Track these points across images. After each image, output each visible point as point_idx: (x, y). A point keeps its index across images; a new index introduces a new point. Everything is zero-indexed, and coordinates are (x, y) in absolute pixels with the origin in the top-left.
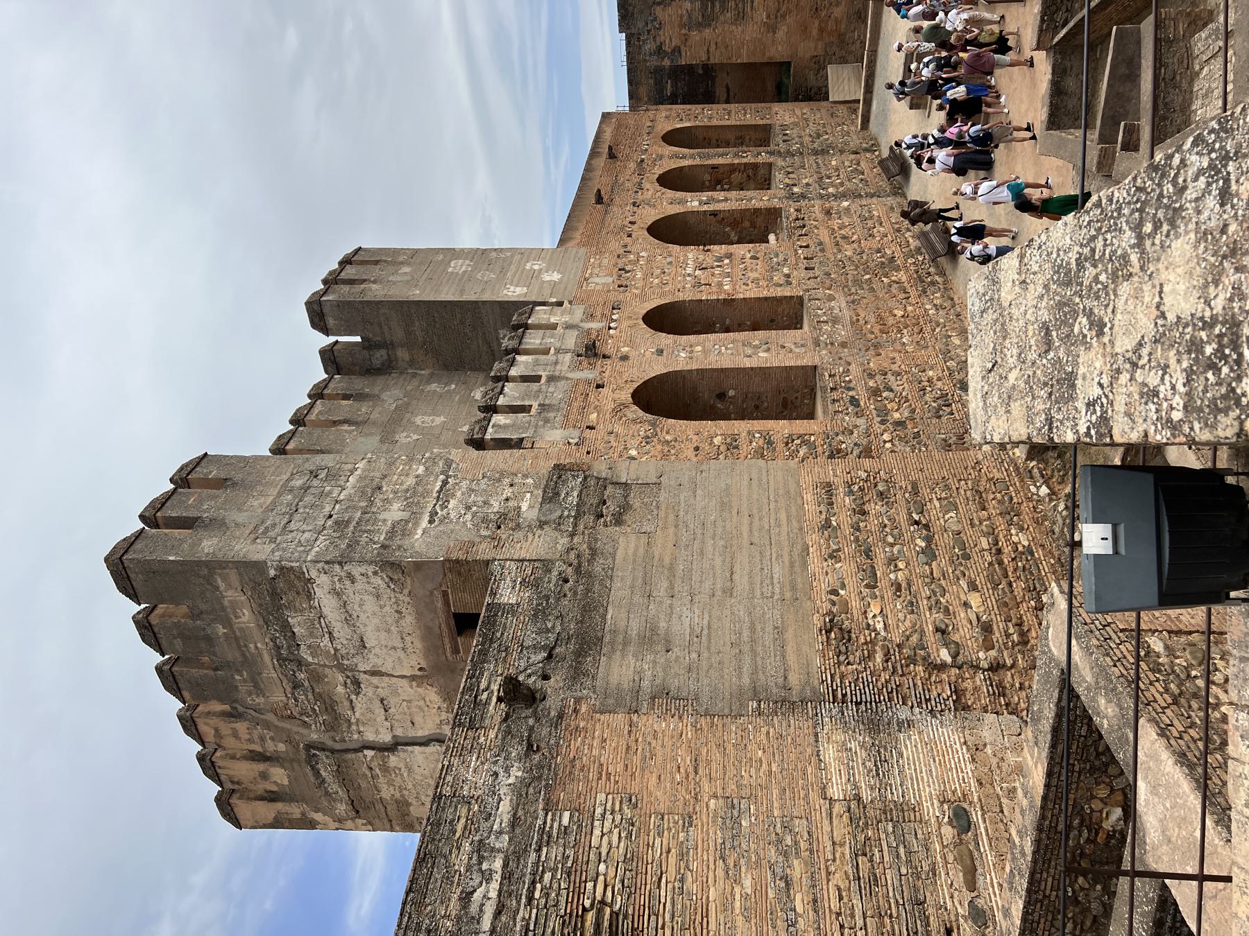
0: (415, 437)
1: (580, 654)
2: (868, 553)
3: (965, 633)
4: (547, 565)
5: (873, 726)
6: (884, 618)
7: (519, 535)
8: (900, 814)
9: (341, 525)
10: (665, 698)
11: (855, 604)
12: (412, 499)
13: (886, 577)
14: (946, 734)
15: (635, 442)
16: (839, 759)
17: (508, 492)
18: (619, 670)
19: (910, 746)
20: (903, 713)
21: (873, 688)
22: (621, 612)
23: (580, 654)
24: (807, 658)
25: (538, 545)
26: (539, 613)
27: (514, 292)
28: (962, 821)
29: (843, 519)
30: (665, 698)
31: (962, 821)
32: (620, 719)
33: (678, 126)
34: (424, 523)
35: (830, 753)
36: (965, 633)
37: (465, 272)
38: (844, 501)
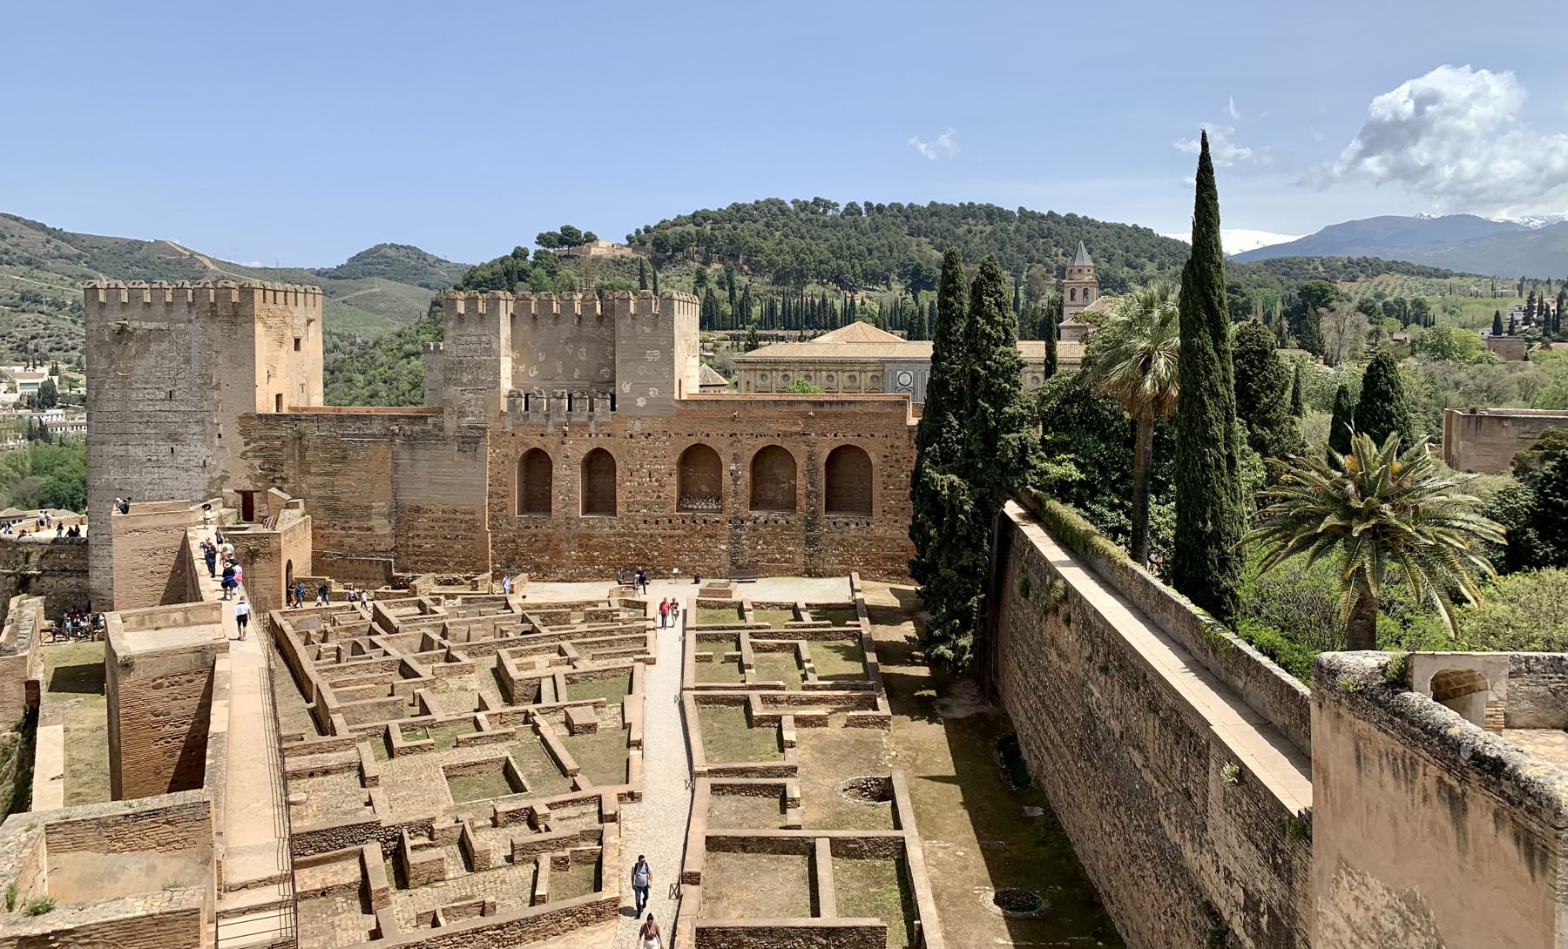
3: (417, 541)
4: (441, 430)
5: (390, 514)
6: (423, 521)
8: (369, 517)
9: (461, 362)
10: (396, 466)
12: (475, 381)
14: (387, 530)
15: (504, 451)
16: (381, 506)
18: (405, 455)
19: (385, 521)
21: (402, 516)
22: (420, 453)
24: (408, 498)
26: (423, 431)
27: (624, 387)
28: (369, 529)
29: (459, 516)
30: (396, 466)
31: (369, 529)
33: (872, 456)
36: (417, 541)
38: (468, 517)
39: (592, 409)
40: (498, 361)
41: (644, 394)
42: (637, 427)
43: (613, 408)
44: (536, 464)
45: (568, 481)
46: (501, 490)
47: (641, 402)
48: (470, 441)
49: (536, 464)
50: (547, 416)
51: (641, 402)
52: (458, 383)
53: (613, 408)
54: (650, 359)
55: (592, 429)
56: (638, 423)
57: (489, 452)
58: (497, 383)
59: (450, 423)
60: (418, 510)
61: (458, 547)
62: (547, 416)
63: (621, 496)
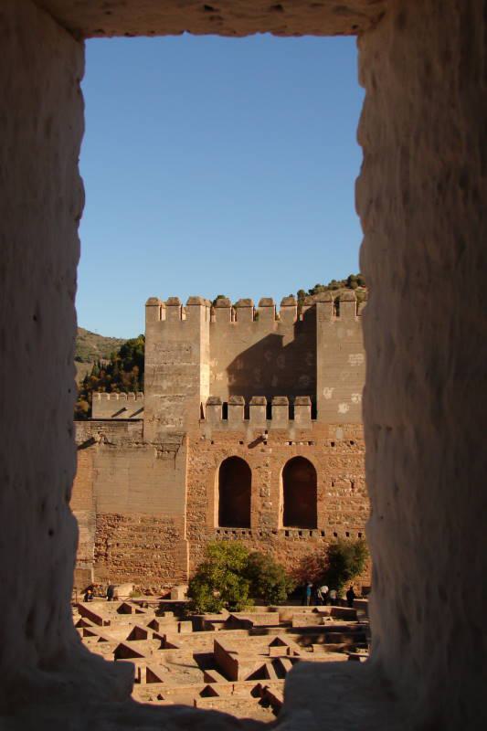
0: (269, 359)
1: (110, 451)
2: (143, 531)
3: (116, 550)
6: (122, 530)
7: (155, 427)
9: (161, 369)
11: (125, 524)
13: (136, 534)
17: (176, 419)
20: (94, 530)
23: (110, 451)
24: (107, 508)
25: (150, 435)
27: (325, 393)
29: (157, 525)
32: (91, 463)
34: (160, 396)
35: (83, 512)
36: (116, 550)
37: (349, 364)
39: (292, 416)
40: (197, 369)
41: (347, 400)
42: (339, 435)
43: (314, 416)
44: (235, 475)
45: (269, 493)
46: (199, 499)
47: (343, 408)
48: (170, 448)
49: (235, 475)
50: (246, 424)
51: (343, 408)
52: (158, 389)
53: (314, 416)
54: (353, 363)
55: (292, 435)
56: (340, 430)
57: (189, 459)
58: (196, 390)
59: (151, 432)
60: (119, 517)
61: (157, 556)
62: (246, 424)
63: (322, 508)
